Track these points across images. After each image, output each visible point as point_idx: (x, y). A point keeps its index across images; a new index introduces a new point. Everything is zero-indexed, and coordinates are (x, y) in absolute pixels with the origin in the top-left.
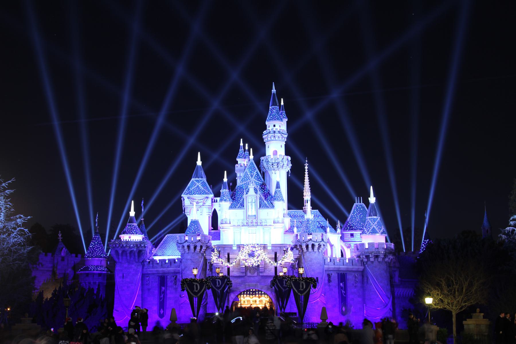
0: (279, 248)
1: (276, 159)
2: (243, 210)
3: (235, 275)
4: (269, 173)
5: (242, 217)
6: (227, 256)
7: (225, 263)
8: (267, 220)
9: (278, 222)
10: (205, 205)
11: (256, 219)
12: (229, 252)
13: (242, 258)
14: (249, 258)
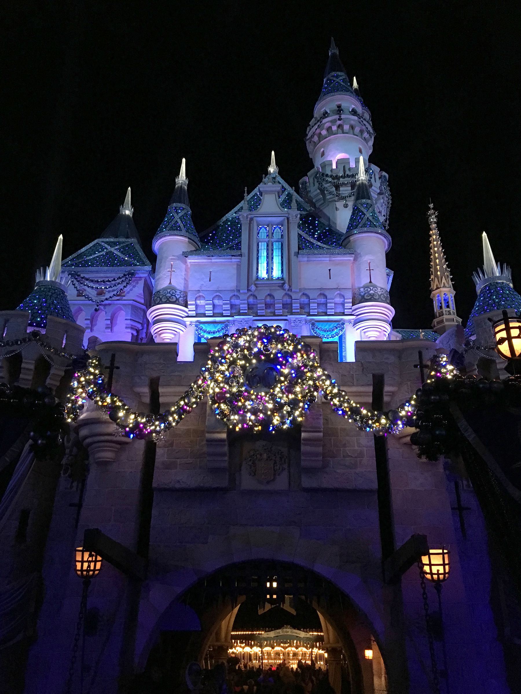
0: (392, 359)
1: (347, 169)
2: (235, 260)
3: (177, 486)
4: (328, 214)
5: (232, 284)
6: (146, 390)
7: (127, 416)
8: (327, 293)
9: (372, 299)
10: (124, 298)
11: (287, 286)
12: (155, 375)
13: (213, 389)
14: (246, 391)
